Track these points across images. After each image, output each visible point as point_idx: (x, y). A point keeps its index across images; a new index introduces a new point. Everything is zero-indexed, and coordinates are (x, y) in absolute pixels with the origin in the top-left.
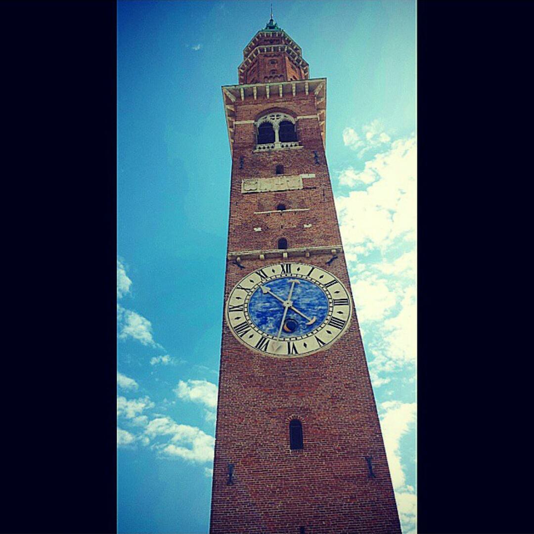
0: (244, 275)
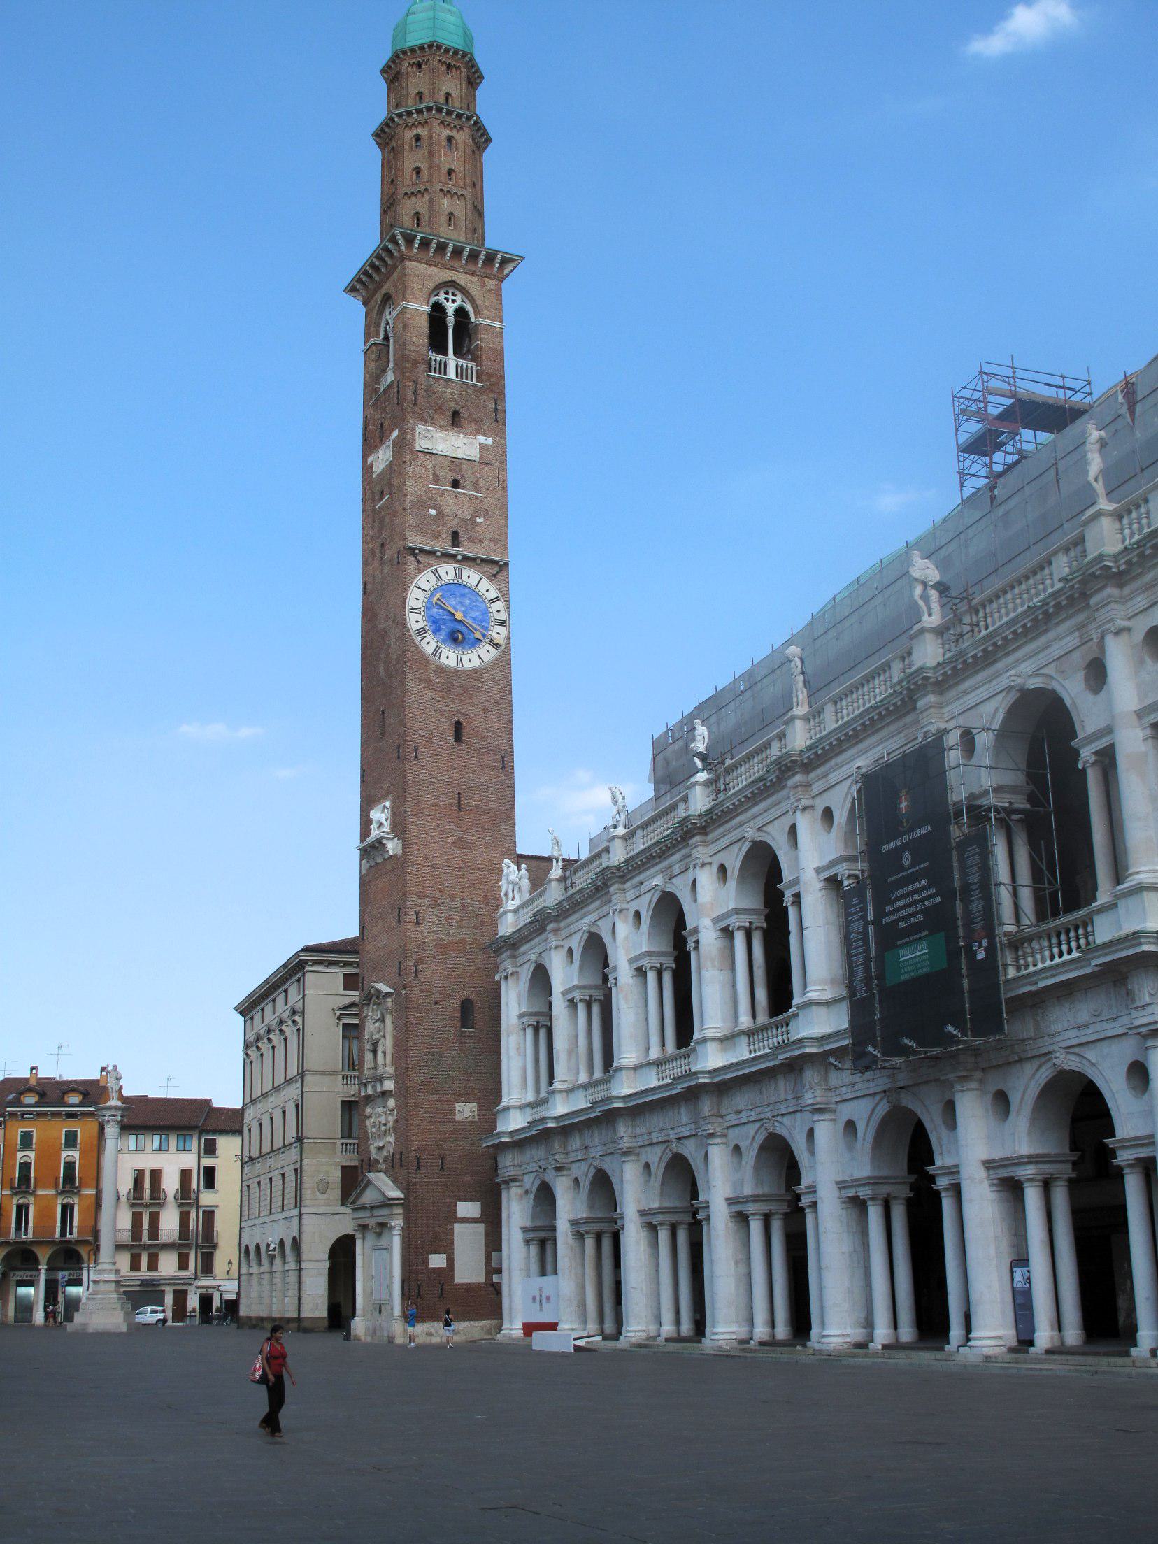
0: (420, 571)
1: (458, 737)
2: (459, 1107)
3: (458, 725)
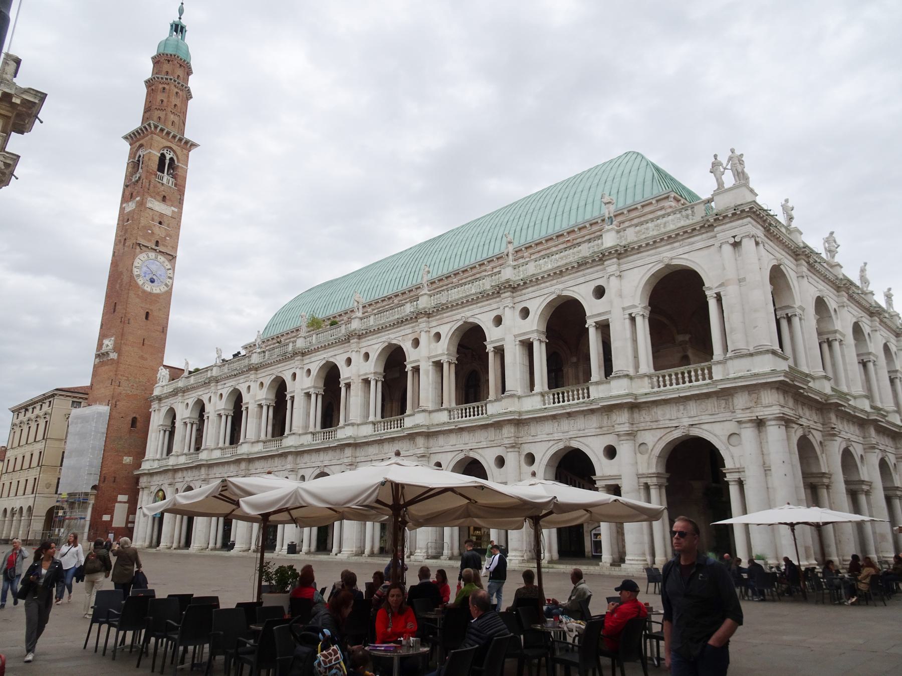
1: (147, 318)
2: (125, 458)
3: (147, 313)
